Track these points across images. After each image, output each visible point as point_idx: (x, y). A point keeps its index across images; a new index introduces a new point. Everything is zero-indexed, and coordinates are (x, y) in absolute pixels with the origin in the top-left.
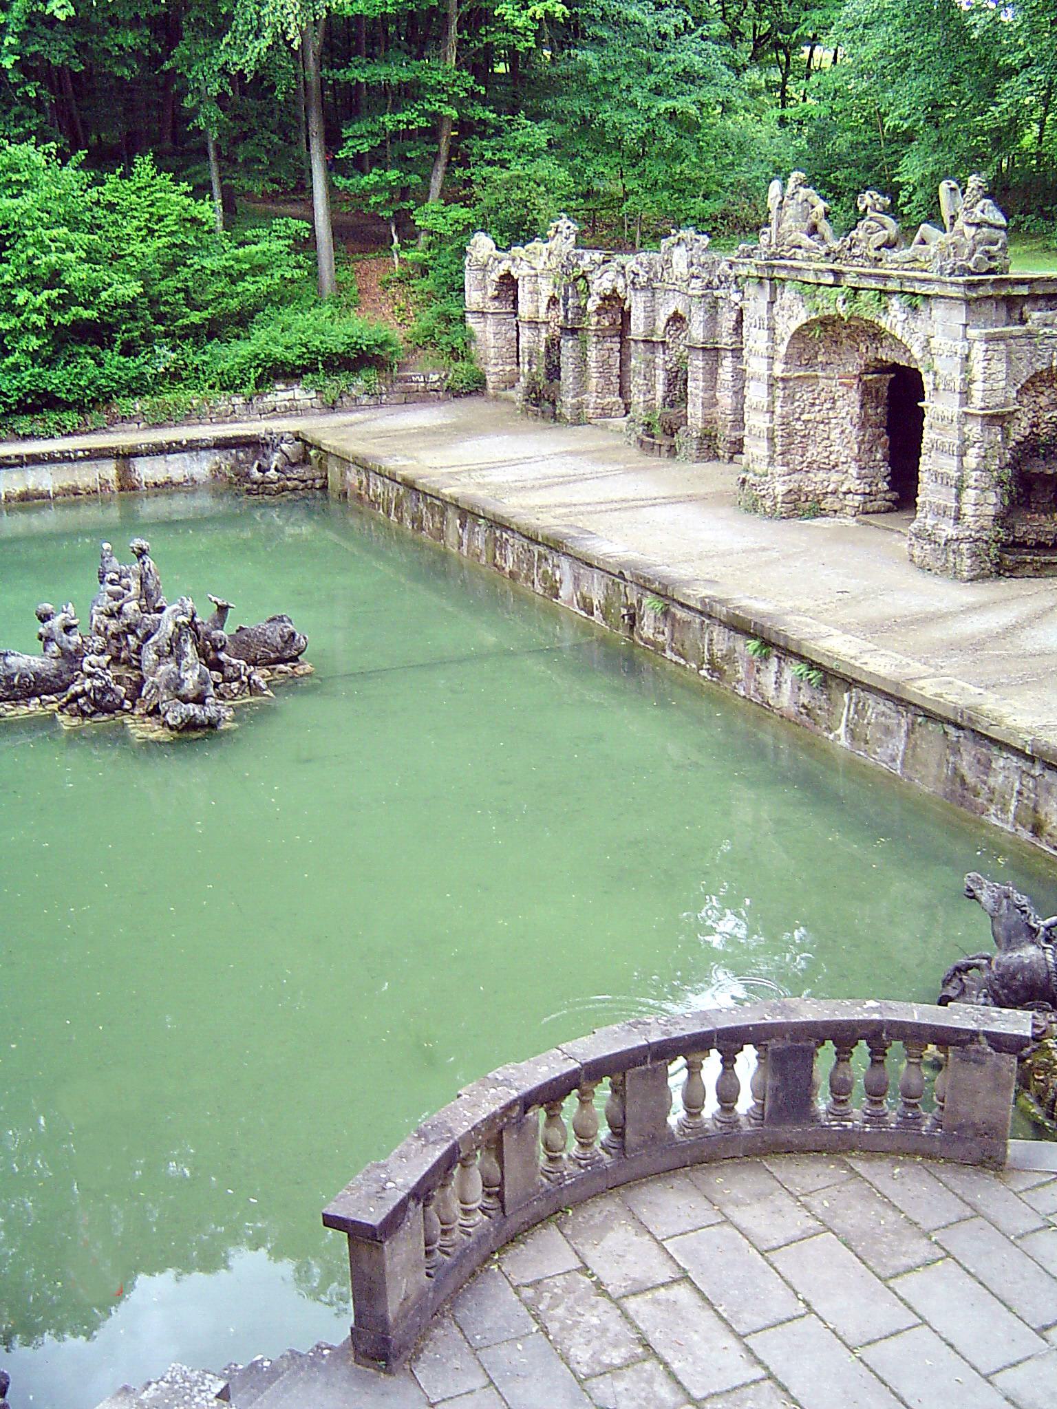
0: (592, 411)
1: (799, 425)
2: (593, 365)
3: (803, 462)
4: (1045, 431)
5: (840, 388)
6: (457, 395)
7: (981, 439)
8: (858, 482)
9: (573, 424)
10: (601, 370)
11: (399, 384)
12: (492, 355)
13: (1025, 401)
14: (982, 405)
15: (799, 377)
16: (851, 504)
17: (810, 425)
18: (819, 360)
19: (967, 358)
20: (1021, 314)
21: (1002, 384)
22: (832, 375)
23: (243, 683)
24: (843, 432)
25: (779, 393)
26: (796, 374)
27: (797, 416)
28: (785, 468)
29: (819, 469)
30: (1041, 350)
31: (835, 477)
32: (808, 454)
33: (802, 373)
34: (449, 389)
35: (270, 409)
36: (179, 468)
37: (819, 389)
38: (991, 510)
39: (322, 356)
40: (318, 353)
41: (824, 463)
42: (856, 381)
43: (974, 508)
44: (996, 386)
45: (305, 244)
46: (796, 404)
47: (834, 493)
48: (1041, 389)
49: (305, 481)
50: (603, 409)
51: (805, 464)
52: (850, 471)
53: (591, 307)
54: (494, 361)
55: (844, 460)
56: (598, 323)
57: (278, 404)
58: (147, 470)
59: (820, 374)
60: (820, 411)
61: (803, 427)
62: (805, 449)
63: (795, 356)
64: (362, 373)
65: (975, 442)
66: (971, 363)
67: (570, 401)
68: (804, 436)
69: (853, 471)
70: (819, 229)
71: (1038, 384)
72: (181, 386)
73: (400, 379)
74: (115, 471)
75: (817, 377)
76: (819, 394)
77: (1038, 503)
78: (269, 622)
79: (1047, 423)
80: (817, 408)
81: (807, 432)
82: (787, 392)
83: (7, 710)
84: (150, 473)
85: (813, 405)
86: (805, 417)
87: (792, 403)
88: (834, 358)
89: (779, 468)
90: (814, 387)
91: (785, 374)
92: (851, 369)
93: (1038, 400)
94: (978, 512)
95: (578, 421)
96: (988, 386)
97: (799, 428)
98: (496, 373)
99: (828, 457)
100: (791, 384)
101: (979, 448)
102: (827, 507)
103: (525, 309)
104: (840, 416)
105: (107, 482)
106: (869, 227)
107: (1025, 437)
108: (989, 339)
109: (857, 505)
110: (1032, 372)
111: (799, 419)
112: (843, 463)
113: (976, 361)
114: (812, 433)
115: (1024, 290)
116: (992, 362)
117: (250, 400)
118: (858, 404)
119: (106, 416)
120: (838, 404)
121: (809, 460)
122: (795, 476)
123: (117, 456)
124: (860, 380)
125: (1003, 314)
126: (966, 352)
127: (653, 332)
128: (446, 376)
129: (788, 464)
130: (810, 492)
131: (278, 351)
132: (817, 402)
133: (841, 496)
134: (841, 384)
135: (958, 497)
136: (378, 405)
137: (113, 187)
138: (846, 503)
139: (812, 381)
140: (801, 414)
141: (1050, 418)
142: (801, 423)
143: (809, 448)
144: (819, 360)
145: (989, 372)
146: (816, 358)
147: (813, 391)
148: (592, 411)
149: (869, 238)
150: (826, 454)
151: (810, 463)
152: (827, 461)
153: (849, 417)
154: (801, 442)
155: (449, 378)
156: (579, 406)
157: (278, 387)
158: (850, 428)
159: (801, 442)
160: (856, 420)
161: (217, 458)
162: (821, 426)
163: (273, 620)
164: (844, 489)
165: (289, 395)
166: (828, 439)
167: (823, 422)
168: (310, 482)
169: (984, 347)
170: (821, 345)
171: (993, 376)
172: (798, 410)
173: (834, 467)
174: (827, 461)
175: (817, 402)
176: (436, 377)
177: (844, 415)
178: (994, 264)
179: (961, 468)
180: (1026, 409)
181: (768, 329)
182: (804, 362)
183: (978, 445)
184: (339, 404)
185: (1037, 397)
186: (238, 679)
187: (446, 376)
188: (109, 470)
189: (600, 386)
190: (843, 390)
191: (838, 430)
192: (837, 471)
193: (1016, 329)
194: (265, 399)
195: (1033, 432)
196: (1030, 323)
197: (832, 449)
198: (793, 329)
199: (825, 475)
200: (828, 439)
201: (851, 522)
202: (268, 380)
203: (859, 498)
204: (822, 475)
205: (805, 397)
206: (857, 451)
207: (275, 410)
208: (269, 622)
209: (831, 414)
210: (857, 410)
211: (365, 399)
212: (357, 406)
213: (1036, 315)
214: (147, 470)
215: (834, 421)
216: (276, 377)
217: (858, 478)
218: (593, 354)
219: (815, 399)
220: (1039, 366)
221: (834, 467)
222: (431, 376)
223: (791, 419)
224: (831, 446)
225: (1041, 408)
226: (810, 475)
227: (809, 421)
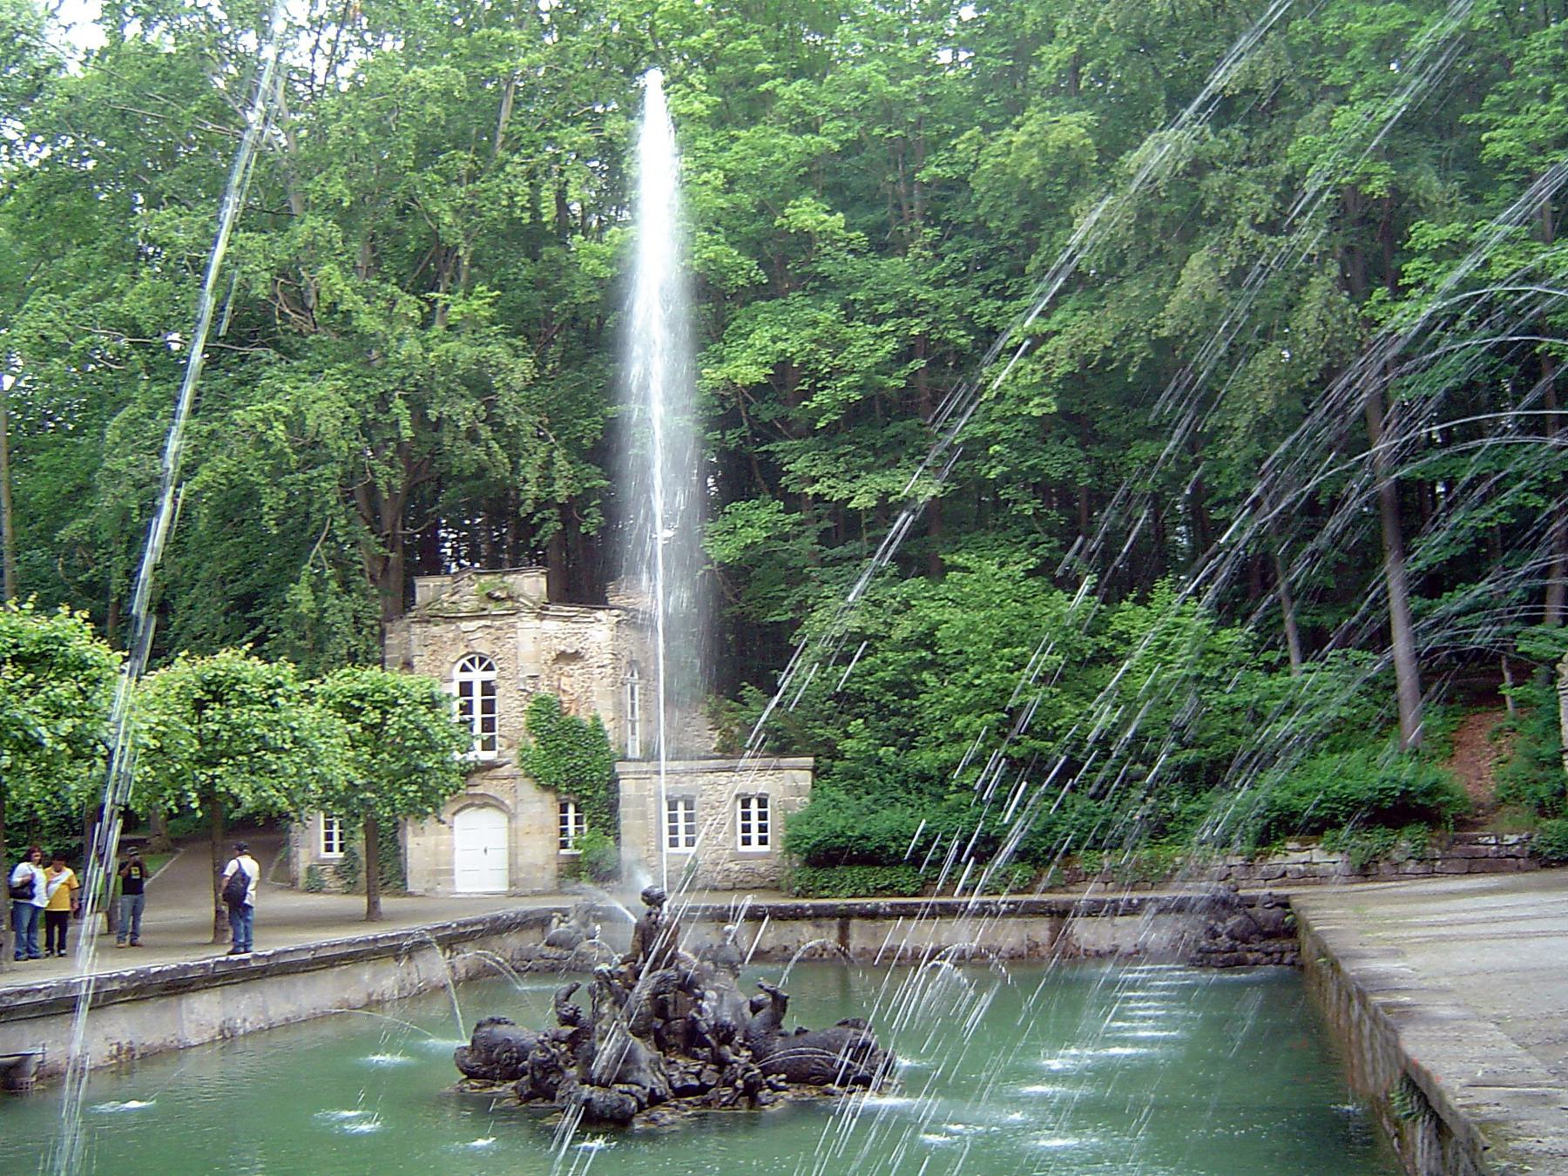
6: (1547, 864)
11: (1460, 847)
23: (736, 1089)
34: (1533, 855)
35: (1279, 873)
36: (1130, 935)
39: (1347, 805)
40: (1339, 800)
45: (1385, 686)
49: (1270, 954)
57: (1290, 867)
58: (1085, 933)
64: (1407, 831)
72: (1165, 840)
73: (1462, 841)
74: (1048, 933)
78: (839, 1025)
83: (473, 1088)
84: (1092, 938)
105: (1037, 945)
117: (1252, 861)
119: (1066, 872)
123: (1052, 913)
128: (1529, 838)
131: (1281, 796)
136: (1431, 874)
137: (1127, 615)
155: (1534, 840)
157: (1290, 845)
161: (1180, 925)
163: (845, 1023)
165: (1304, 856)
168: (1276, 956)
176: (1513, 839)
184: (1374, 871)
186: (731, 1084)
187: (1529, 838)
188: (1040, 930)
194: (1270, 860)
202: (1277, 838)
207: (1284, 875)
208: (839, 1025)
211: (1411, 866)
212: (1398, 873)
214: (1085, 933)
216: (1290, 832)
222: (1506, 837)
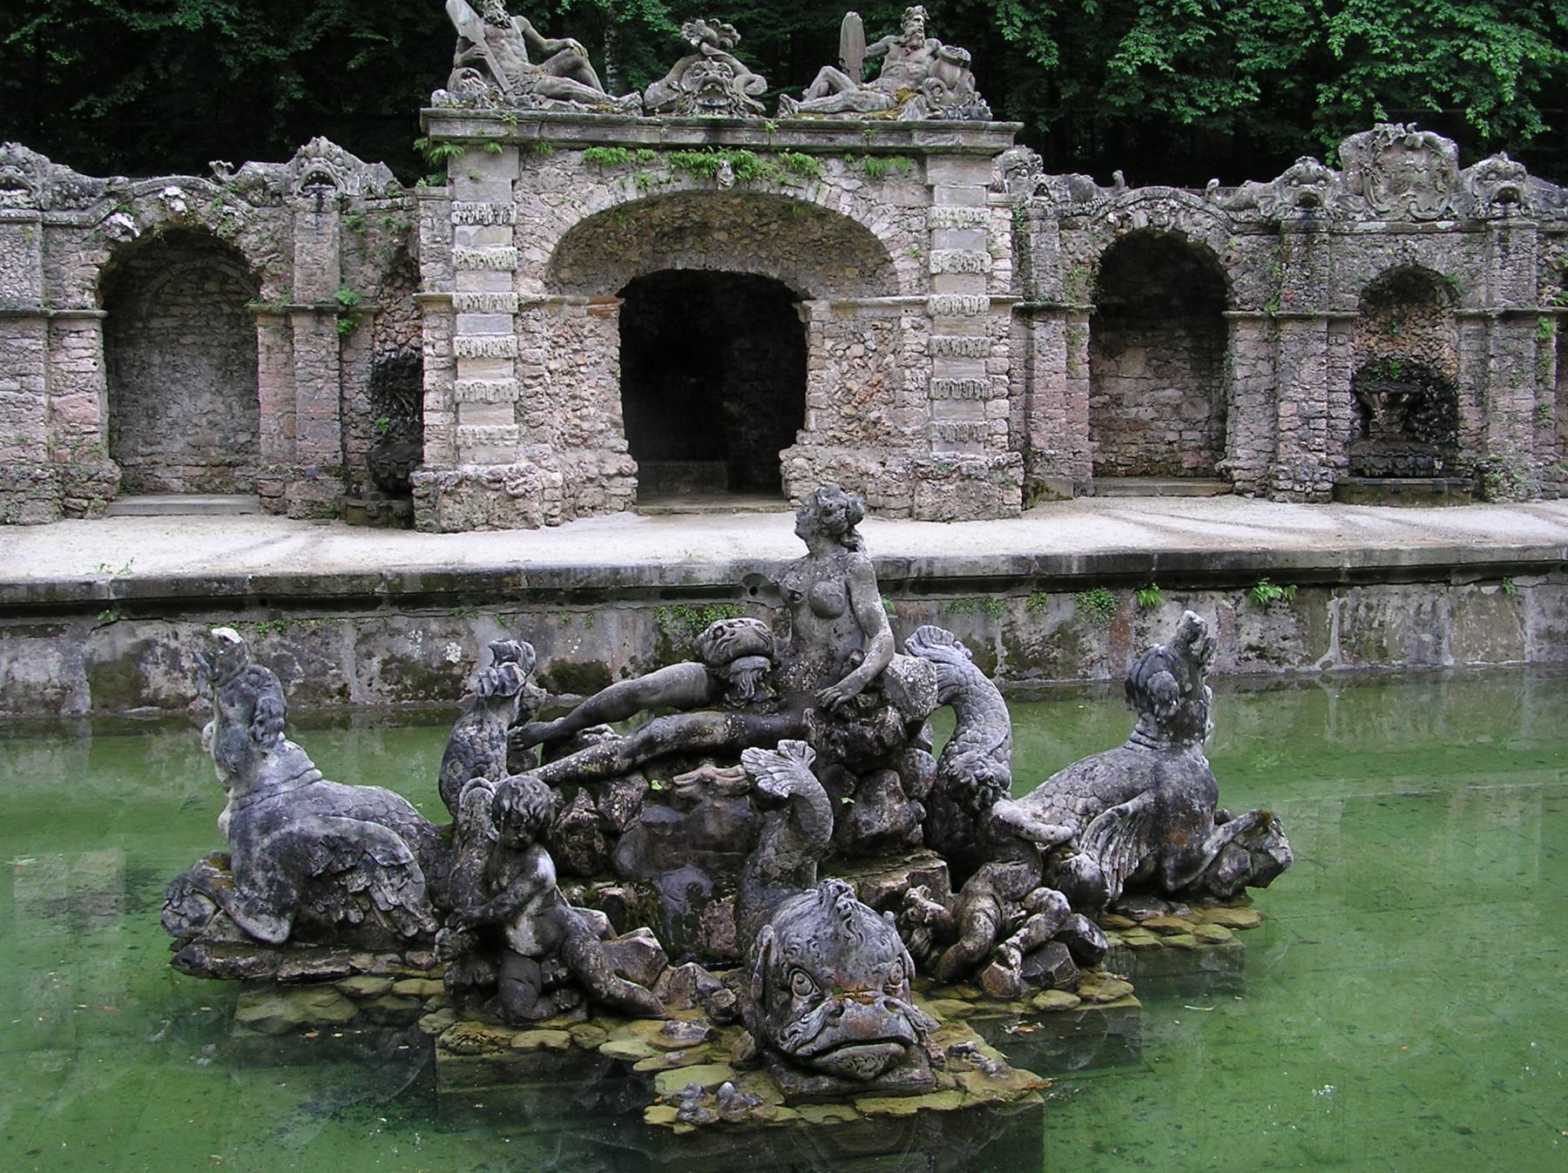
16: (619, 491)
31: (589, 456)
41: (572, 436)
55: (602, 426)
104: (592, 360)
112: (601, 432)
134: (590, 313)
138: (614, 491)
162: (567, 380)
166: (574, 397)
190: (590, 323)
192: (588, 447)
197: (585, 411)
201: (629, 516)
215: (583, 369)
219: (559, 336)
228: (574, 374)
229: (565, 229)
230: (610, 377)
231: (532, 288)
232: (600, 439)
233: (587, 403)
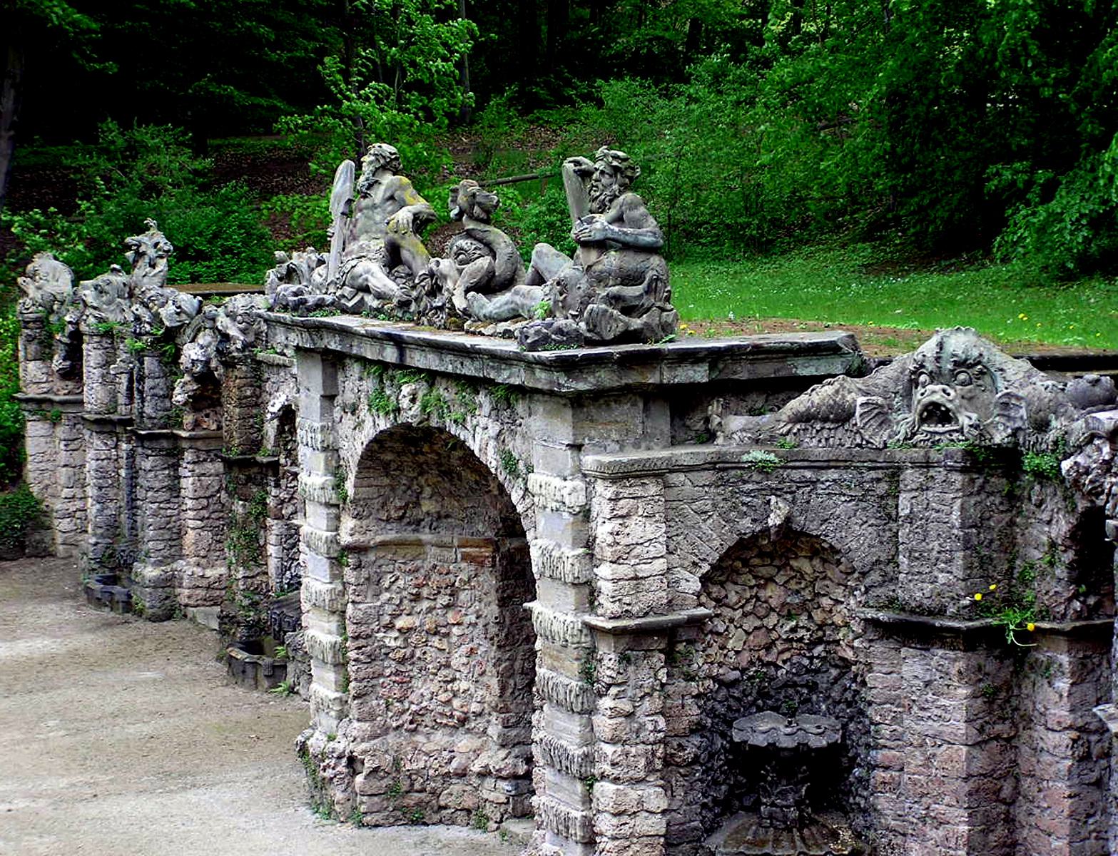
0: (186, 592)
1: (391, 640)
2: (190, 503)
3: (404, 712)
4: (786, 656)
5: (463, 565)
7: (620, 679)
8: (503, 753)
9: (155, 619)
10: (205, 513)
12: (63, 480)
13: (733, 598)
14: (616, 608)
15: (383, 544)
17: (413, 638)
18: (425, 509)
19: (585, 514)
20: (707, 420)
21: (660, 565)
22: (447, 539)
24: (472, 652)
25: (350, 575)
26: (379, 539)
27: (387, 619)
28: (366, 726)
29: (437, 726)
30: (748, 494)
31: (464, 743)
32: (413, 697)
33: (391, 536)
37: (427, 565)
38: (656, 825)
42: (487, 552)
43: (615, 821)
44: (644, 570)
46: (386, 596)
47: (462, 774)
48: (764, 571)
50: (208, 588)
51: (407, 717)
52: (490, 731)
53: (179, 397)
54: (66, 492)
55: (474, 707)
56: (197, 424)
59: (426, 536)
60: (430, 610)
61: (399, 643)
62: (405, 683)
63: (376, 503)
65: (609, 686)
66: (593, 525)
67: (150, 572)
68: (402, 661)
69: (494, 730)
70: (405, 254)
71: (756, 561)
75: (420, 544)
76: (427, 577)
77: (773, 805)
79: (789, 640)
80: (425, 605)
81: (408, 651)
82: (364, 573)
85: (417, 598)
86: (400, 623)
87: (377, 595)
88: (452, 505)
89: (356, 724)
90: (419, 563)
91: (356, 537)
92: (480, 527)
93: (762, 594)
94: (626, 830)
95: (169, 612)
96: (623, 570)
97: (393, 644)
98: (71, 515)
99: (448, 702)
100: (372, 557)
101: (617, 697)
102: (451, 801)
103: (94, 395)
104: (467, 620)
106: (461, 250)
107: (743, 671)
108: (619, 476)
109: (503, 799)
110: (732, 540)
111: (390, 627)
113: (600, 520)
114: (418, 653)
115: (699, 374)
116: (630, 522)
118: (493, 597)
120: (463, 596)
121: (414, 708)
122: (391, 738)
124: (497, 550)
125: (662, 423)
126: (582, 501)
127: (257, 445)
129: (371, 717)
130: (418, 772)
132: (425, 592)
133: (475, 781)
134: (463, 559)
135: (588, 799)
139: (411, 552)
140: (395, 616)
141: (793, 630)
142: (396, 634)
143: (415, 683)
144: (425, 509)
145: (624, 541)
146: (417, 504)
147: (417, 570)
148: (186, 592)
149: (460, 272)
150: (443, 697)
151: (416, 713)
152: (447, 710)
153: (481, 622)
154: (397, 673)
156: (169, 583)
158: (486, 644)
159: (397, 673)
160: (493, 630)
162: (435, 641)
164: (476, 768)
166: (448, 666)
167: (435, 634)
169: (609, 493)
170: (422, 480)
171: (638, 550)
172: (389, 609)
173: (463, 721)
174: (447, 710)
175: (425, 592)
177: (473, 618)
178: (636, 323)
179: (590, 738)
180: (739, 613)
181: (325, 449)
182: (394, 515)
183: (614, 691)
185: (759, 586)
189: (204, 544)
190: (466, 569)
191: (464, 649)
192: (469, 731)
193: (685, 454)
195: (759, 659)
196: (720, 441)
197: (455, 686)
198: (360, 449)
199: (447, 738)
200: (448, 666)
203: (505, 785)
204: (440, 738)
205: (401, 583)
206: (498, 692)
209: (451, 617)
210: (494, 610)
213: (737, 423)
215: (455, 630)
217: (503, 746)
218: (187, 484)
219: (419, 586)
220: (746, 525)
221: (463, 721)
223: (374, 626)
224: (453, 680)
225: (772, 609)
226: (420, 738)
227: (409, 629)
228: (447, 635)
229: (357, 458)
230: (486, 644)
231: (348, 530)
232: (479, 724)
233: (458, 675)
